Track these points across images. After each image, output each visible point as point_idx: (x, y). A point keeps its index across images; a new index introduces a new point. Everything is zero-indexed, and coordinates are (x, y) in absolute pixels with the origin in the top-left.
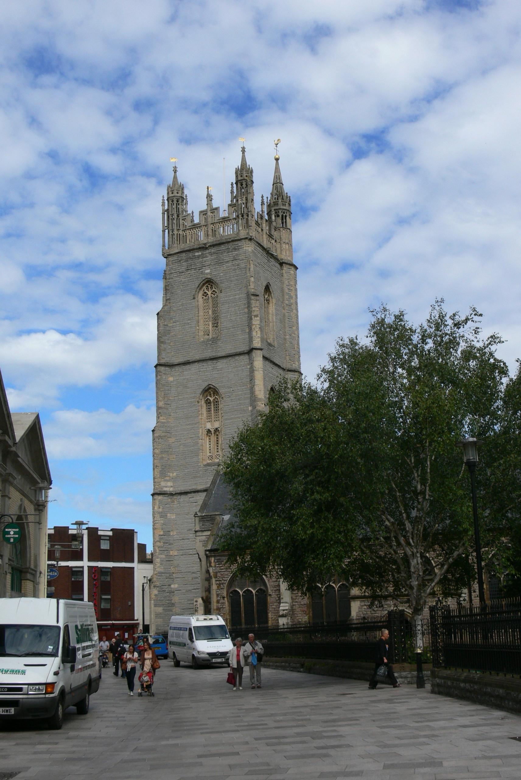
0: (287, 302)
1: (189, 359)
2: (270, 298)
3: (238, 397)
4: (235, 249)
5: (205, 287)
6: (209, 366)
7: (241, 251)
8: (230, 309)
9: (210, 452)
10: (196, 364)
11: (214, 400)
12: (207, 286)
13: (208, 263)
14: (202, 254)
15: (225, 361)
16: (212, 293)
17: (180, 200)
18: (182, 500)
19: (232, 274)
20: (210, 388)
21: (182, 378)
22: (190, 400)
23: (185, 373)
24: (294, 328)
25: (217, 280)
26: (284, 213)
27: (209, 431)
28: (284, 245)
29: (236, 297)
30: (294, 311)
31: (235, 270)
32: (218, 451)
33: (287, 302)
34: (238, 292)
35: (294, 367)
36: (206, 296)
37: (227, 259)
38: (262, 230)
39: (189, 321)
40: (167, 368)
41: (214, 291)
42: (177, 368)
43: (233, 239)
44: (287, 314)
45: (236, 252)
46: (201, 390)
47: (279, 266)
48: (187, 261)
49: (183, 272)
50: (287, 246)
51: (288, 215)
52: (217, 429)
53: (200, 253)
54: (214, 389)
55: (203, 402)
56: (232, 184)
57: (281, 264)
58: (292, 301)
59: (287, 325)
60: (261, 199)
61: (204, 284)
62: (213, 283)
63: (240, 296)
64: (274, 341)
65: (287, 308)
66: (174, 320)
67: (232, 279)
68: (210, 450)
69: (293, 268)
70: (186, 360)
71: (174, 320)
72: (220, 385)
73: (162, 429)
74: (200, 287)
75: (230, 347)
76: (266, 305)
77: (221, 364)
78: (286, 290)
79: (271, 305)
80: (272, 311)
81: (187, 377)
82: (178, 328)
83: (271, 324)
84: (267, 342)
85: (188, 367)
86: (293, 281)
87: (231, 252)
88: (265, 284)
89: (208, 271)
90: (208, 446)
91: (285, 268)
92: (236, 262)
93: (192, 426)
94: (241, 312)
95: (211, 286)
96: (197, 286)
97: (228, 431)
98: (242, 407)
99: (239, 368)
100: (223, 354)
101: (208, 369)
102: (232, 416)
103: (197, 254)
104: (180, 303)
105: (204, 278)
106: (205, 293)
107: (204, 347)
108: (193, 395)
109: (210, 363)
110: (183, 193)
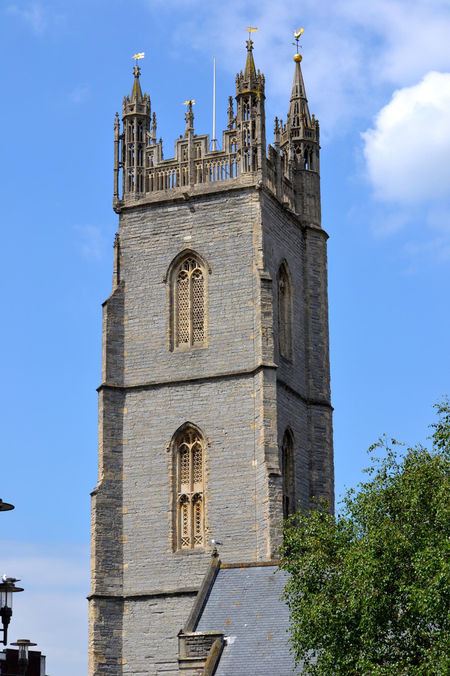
0: (311, 291)
1: (153, 379)
2: (286, 283)
4: (234, 204)
5: (182, 264)
6: (187, 392)
7: (244, 208)
8: (223, 301)
9: (185, 532)
11: (194, 447)
12: (187, 263)
14: (179, 210)
16: (194, 274)
17: (144, 122)
19: (228, 245)
20: (189, 428)
21: (142, 409)
22: (154, 447)
23: (146, 402)
24: (322, 334)
25: (203, 252)
26: (309, 147)
27: (184, 498)
28: (308, 199)
29: (235, 281)
30: (323, 306)
31: (233, 237)
32: (198, 531)
33: (311, 291)
34: (238, 274)
35: (321, 396)
37: (221, 219)
38: (276, 174)
39: (156, 318)
40: (117, 393)
41: (197, 270)
43: (231, 188)
44: (310, 311)
45: (235, 210)
46: (174, 431)
47: (300, 233)
48: (156, 220)
49: (147, 238)
50: (313, 201)
51: (314, 150)
52: (197, 495)
53: (176, 209)
54: (195, 430)
55: (176, 450)
56: (231, 100)
57: (304, 230)
58: (319, 290)
59: (310, 329)
60: (275, 123)
61: (181, 259)
62: (196, 257)
63: (241, 280)
64: (291, 354)
65: (311, 301)
67: (230, 252)
68: (185, 528)
69: (322, 238)
70: (149, 380)
71: (130, 315)
72: (204, 423)
74: (175, 264)
75: (223, 363)
76: (280, 295)
78: (311, 273)
79: (287, 295)
80: (289, 306)
81: (150, 409)
82: (137, 328)
83: (287, 327)
84: (281, 356)
85: (152, 393)
86: (322, 257)
87: (227, 208)
88: (278, 261)
89: (188, 238)
91: (308, 237)
92: (233, 225)
93: (158, 489)
94: (242, 306)
95: (194, 262)
96: (170, 262)
98: (241, 460)
99: (238, 398)
100: (212, 373)
101: (185, 397)
102: (225, 475)
103: (170, 209)
104: (141, 288)
105: (181, 250)
106: (183, 273)
107: (178, 361)
108: (160, 439)
109: (189, 387)
110: (149, 110)
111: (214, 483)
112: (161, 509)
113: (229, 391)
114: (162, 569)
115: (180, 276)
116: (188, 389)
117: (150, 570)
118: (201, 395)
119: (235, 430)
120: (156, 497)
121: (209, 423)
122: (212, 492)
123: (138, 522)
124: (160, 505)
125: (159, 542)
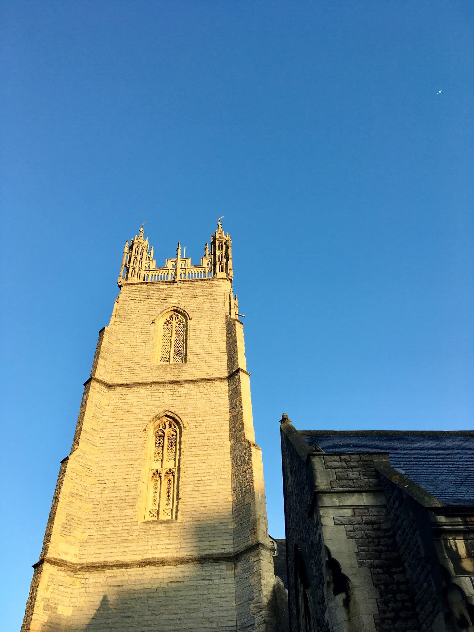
3: (210, 429)
10: (148, 387)
13: (174, 295)
15: (191, 386)
18: (92, 581)
22: (132, 429)
23: (129, 396)
36: (168, 325)
42: (117, 390)
66: (121, 341)
72: (181, 412)
73: (81, 460)
77: (184, 389)
85: (134, 389)
90: (151, 495)
95: (177, 316)
97: (192, 472)
102: (199, 453)
108: (139, 422)
111: (189, 459)
112: (131, 480)
113: (205, 391)
114: (127, 538)
115: (165, 323)
116: (169, 388)
117: (112, 539)
118: (180, 393)
119: (211, 417)
120: (128, 469)
121: (187, 412)
122: (186, 466)
123: (105, 492)
124: (132, 476)
125: (126, 511)
